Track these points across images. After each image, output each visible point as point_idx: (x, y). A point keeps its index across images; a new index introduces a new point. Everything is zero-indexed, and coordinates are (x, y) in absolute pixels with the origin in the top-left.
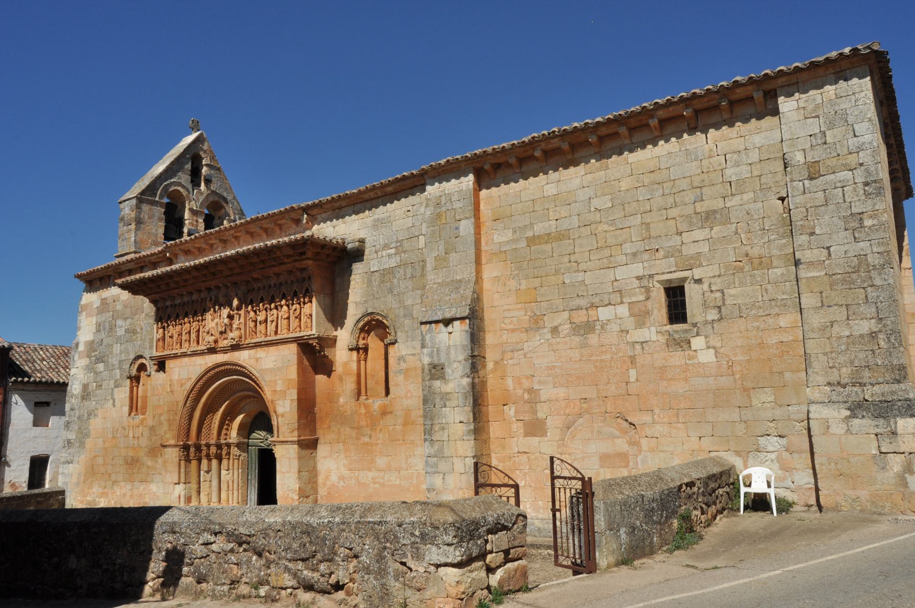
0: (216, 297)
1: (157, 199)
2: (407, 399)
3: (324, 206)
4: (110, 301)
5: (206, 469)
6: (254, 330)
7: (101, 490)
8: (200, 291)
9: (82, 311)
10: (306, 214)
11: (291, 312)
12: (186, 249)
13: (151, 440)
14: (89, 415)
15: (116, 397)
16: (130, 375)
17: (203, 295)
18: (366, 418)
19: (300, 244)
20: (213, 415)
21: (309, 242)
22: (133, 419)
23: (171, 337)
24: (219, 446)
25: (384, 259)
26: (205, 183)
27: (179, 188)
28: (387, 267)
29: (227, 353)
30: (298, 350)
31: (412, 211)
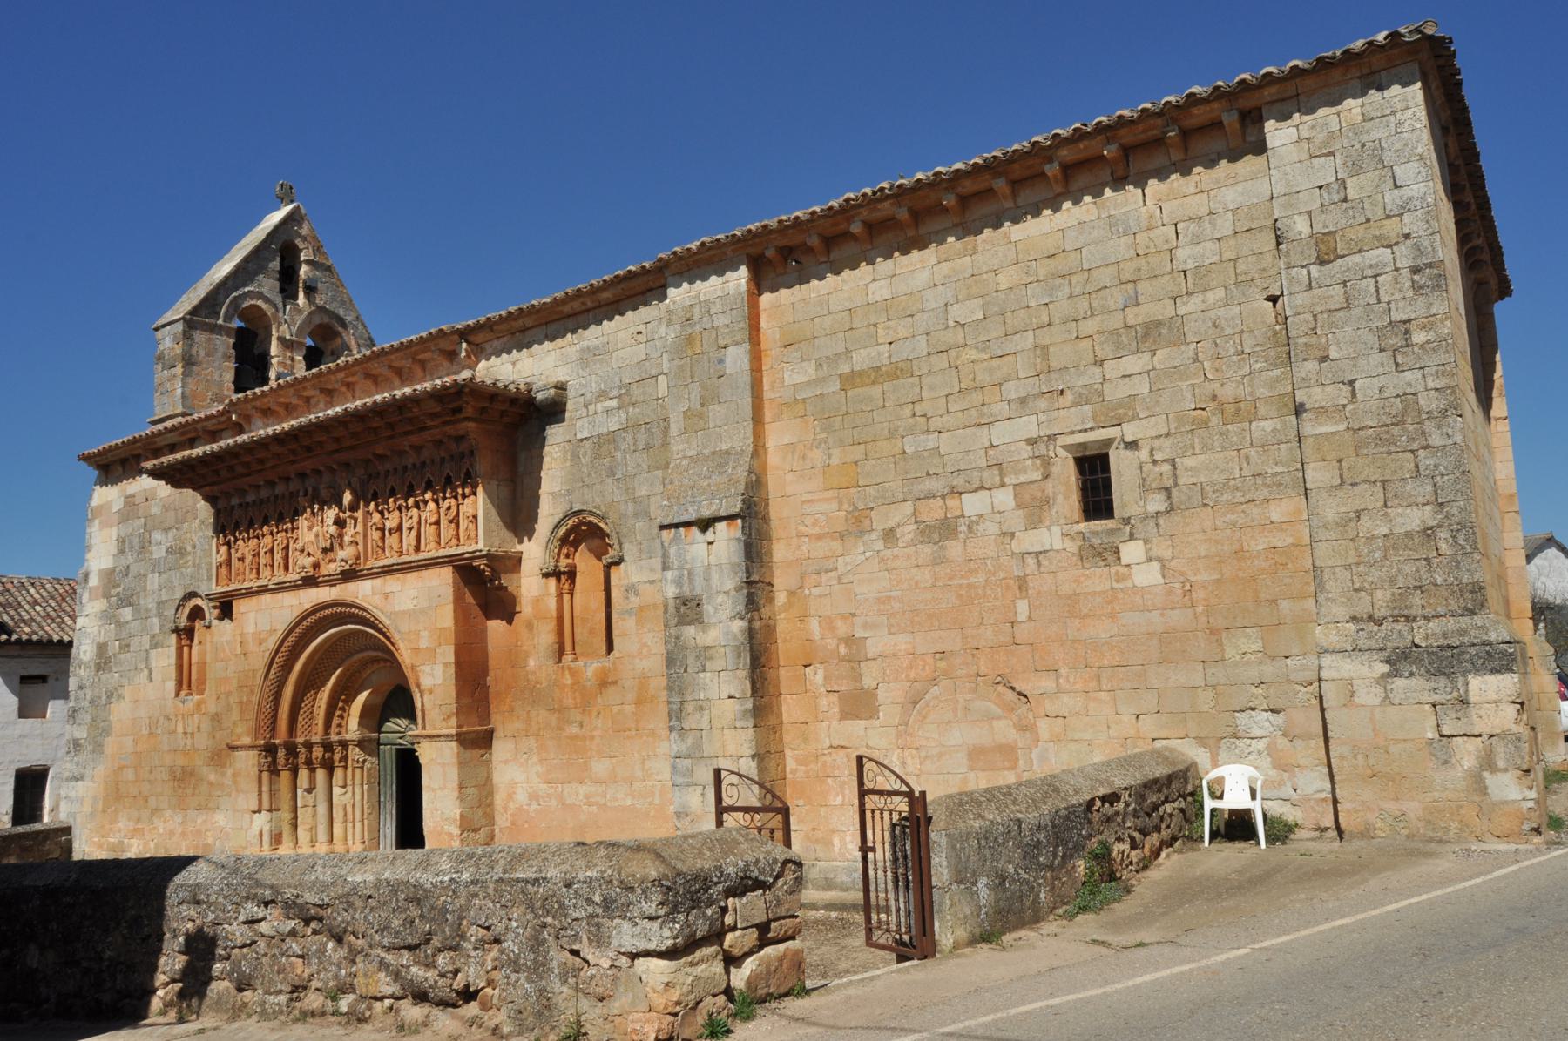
0: (315, 489)
1: (220, 321)
2: (641, 659)
3: (495, 328)
5: (306, 785)
6: (380, 544)
7: (131, 825)
8: (288, 479)
9: (94, 518)
10: (466, 341)
11: (442, 511)
12: (264, 407)
13: (214, 737)
14: (110, 696)
15: (153, 664)
16: (177, 627)
17: (293, 486)
18: (574, 693)
19: (451, 394)
20: (317, 693)
21: (467, 390)
23: (242, 559)
24: (328, 747)
25: (599, 418)
26: (305, 293)
27: (260, 303)
28: (605, 430)
29: (335, 585)
31: (644, 333)
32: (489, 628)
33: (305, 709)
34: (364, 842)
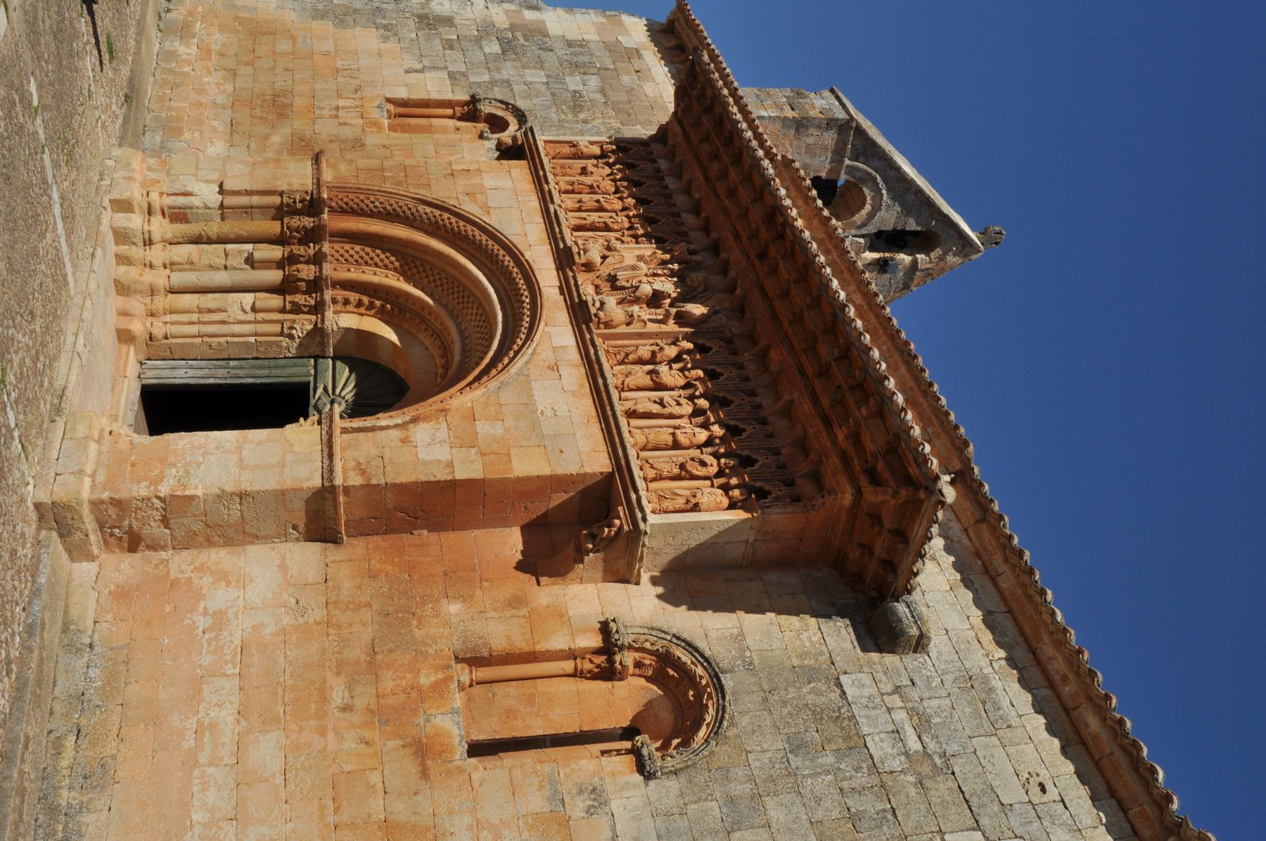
0: (698, 266)
1: (847, 162)
2: (470, 828)
4: (636, 63)
5: (258, 255)
6: (631, 357)
7: (216, 47)
9: (607, 17)
13: (331, 141)
14: (385, 27)
15: (429, 75)
16: (479, 100)
18: (404, 691)
19: (906, 469)
20: (395, 269)
22: (379, 107)
23: (584, 171)
24: (315, 286)
26: (878, 260)
27: (868, 207)
29: (562, 293)
30: (594, 475)
31: (1045, 798)
32: (508, 530)
33: (372, 254)
34: (166, 338)
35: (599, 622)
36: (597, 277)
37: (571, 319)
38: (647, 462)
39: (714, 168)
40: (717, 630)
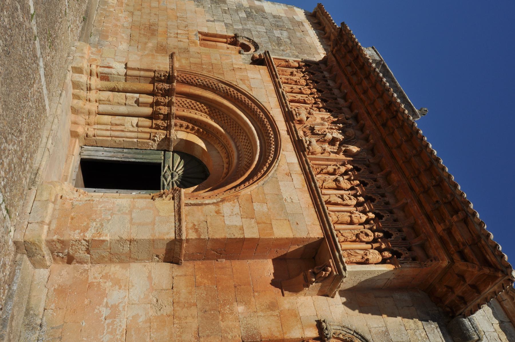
4: (302, 28)
5: (141, 100)
6: (324, 171)
13: (174, 48)
15: (216, 23)
16: (238, 37)
20: (206, 113)
22: (195, 35)
23: (292, 74)
24: (167, 117)
29: (289, 134)
32: (265, 261)
33: (195, 104)
34: (94, 136)
35: (316, 321)
36: (305, 127)
37: (294, 148)
38: (340, 232)
39: (354, 79)
40: (375, 328)
